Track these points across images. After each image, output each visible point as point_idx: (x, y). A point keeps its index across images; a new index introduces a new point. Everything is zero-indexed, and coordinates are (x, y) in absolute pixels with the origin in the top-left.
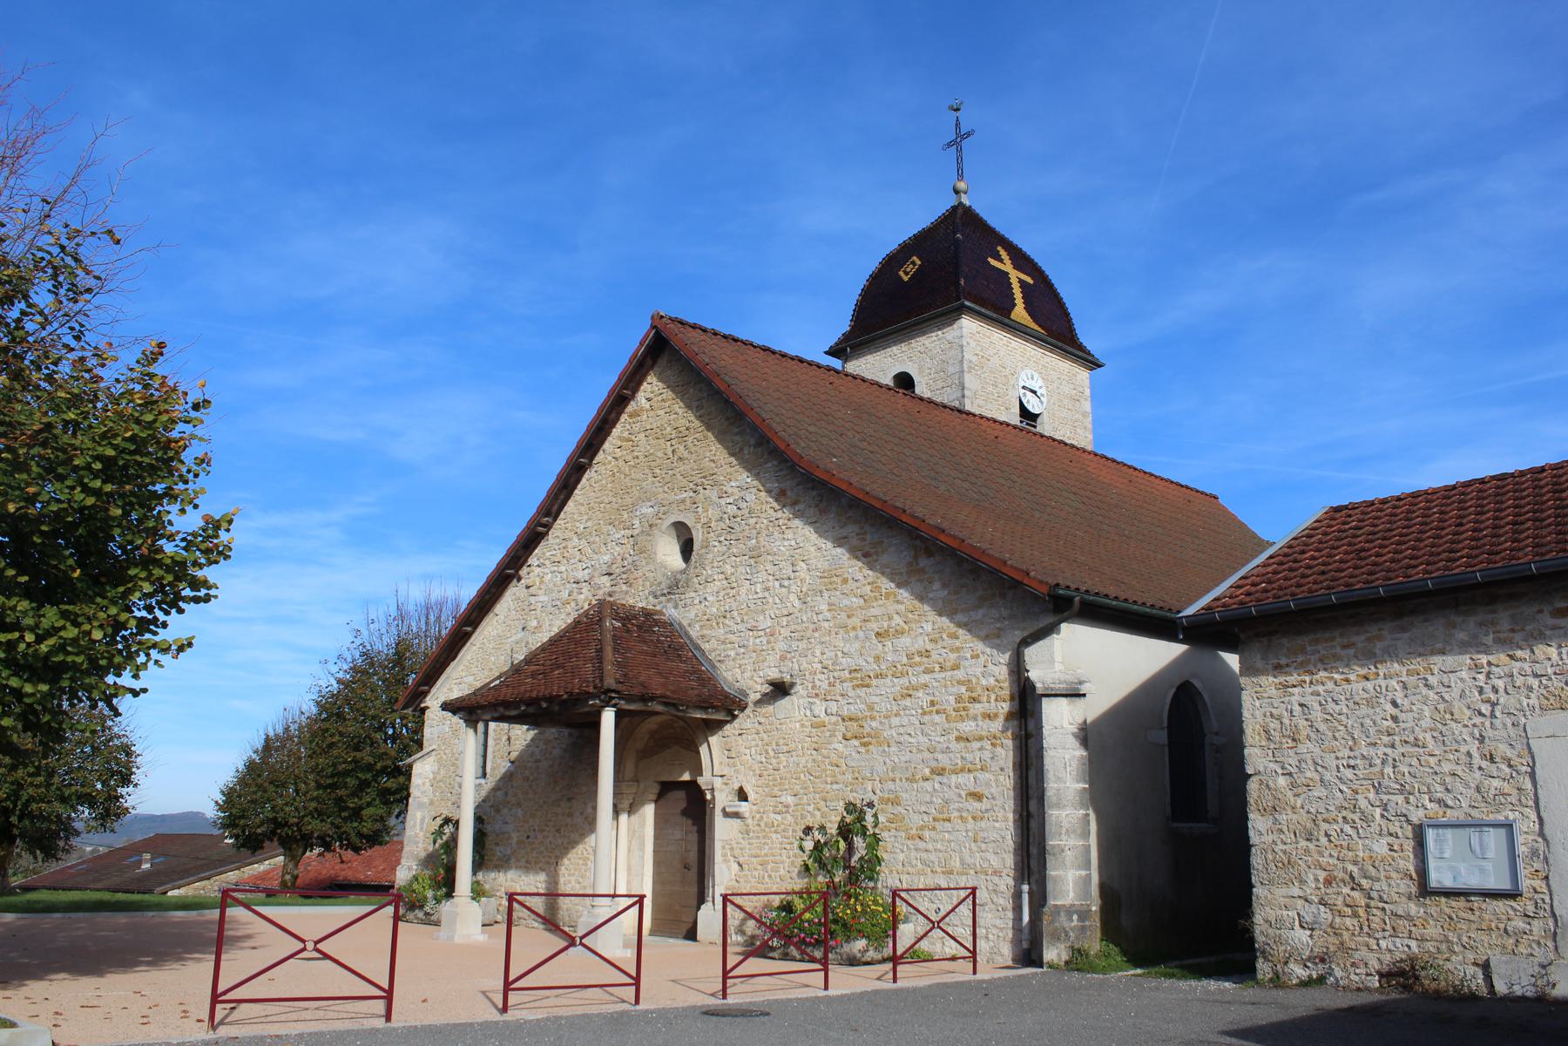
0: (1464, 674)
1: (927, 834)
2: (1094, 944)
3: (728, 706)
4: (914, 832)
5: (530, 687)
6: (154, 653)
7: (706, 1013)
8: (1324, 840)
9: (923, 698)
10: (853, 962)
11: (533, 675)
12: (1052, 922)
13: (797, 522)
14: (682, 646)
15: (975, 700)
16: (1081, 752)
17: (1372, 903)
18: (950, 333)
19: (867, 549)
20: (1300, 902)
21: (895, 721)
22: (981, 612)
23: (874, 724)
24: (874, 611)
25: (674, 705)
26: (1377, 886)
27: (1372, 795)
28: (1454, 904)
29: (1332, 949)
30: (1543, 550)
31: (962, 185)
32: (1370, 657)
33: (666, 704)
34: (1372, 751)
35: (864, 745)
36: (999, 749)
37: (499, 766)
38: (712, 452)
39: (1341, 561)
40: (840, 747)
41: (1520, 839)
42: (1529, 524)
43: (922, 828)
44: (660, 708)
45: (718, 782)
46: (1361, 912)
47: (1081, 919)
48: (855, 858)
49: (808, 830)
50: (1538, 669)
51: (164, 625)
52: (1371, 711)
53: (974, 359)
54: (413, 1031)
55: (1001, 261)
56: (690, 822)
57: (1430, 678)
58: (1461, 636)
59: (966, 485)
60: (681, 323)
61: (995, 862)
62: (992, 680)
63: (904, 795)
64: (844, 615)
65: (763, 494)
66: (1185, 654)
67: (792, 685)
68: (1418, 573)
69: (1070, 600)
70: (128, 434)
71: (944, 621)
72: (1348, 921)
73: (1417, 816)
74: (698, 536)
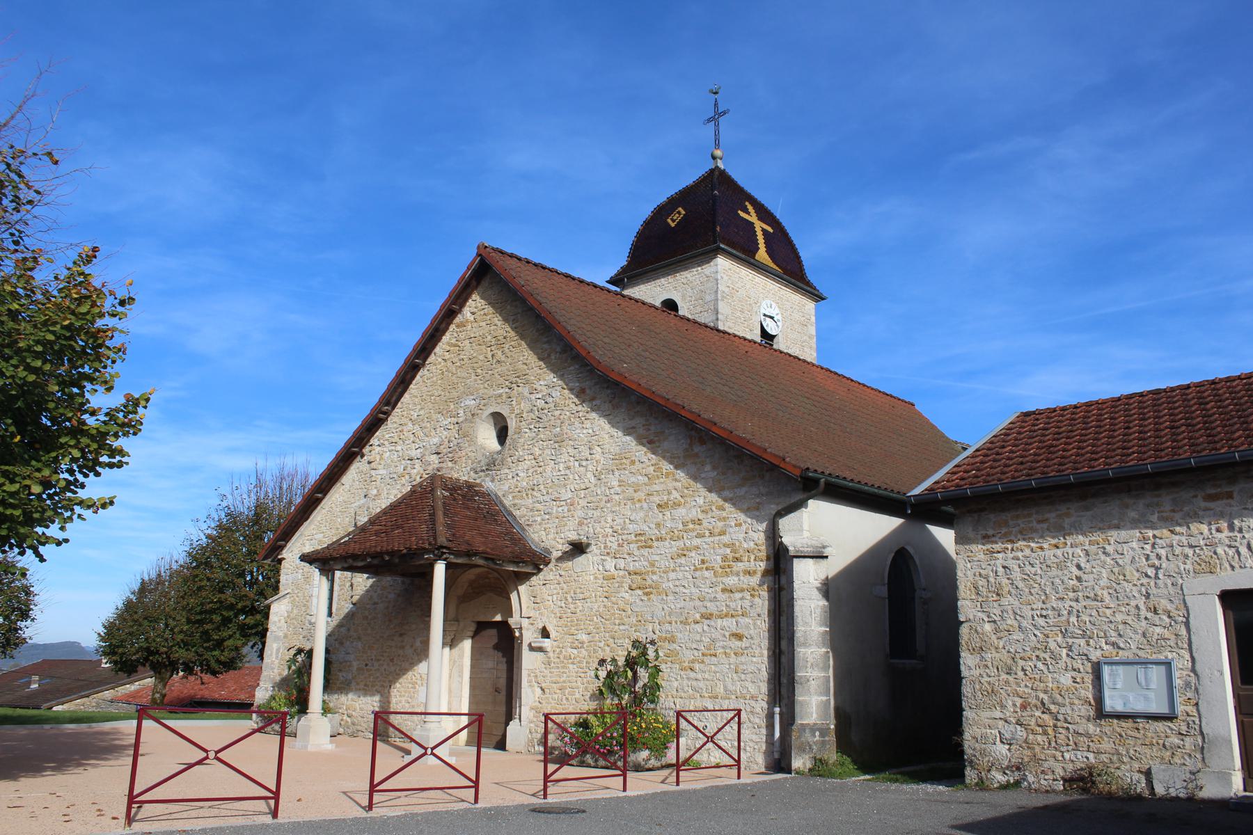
0: (1134, 545)
1: (697, 666)
2: (832, 756)
3: (535, 561)
4: (686, 664)
5: (374, 543)
6: (77, 509)
7: (534, 810)
8: (1021, 674)
9: (695, 557)
10: (638, 768)
11: (377, 533)
12: (799, 737)
13: (594, 415)
14: (498, 512)
15: (737, 560)
16: (824, 603)
17: (1059, 724)
18: (707, 269)
20: (1001, 723)
21: (672, 575)
22: (744, 489)
23: (655, 578)
24: (657, 487)
25: (492, 560)
26: (1063, 710)
27: (1059, 639)
28: (1124, 724)
29: (1026, 759)
30: (1199, 448)
31: (718, 153)
32: (1060, 530)
33: (486, 559)
34: (1060, 604)
35: (647, 594)
36: (757, 600)
37: (343, 607)
38: (525, 357)
39: (1035, 454)
40: (627, 596)
41: (1176, 674)
42: (1184, 428)
43: (693, 661)
44: (481, 562)
45: (525, 623)
46: (1050, 731)
47: (822, 735)
48: (640, 684)
49: (602, 662)
50: (1193, 541)
51: (83, 486)
52: (1060, 573)
53: (727, 290)
54: (297, 827)
55: (748, 213)
56: (500, 654)
57: (1107, 547)
58: (1133, 514)
59: (726, 389)
60: (501, 252)
61: (753, 689)
62: (752, 544)
63: (679, 635)
64: (631, 490)
65: (566, 391)
66: (901, 525)
67: (588, 545)
68: (1099, 465)
69: (817, 481)
70: (66, 323)
71: (713, 497)
72: (1039, 738)
73: (1095, 655)
74: (512, 425)
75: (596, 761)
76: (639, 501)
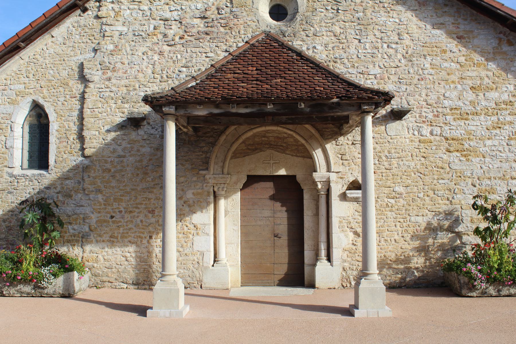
13: (400, 8)
19: (461, 34)
21: (489, 143)
40: (445, 157)
56: (278, 204)
64: (444, 73)
75: (499, 291)
76: (453, 82)
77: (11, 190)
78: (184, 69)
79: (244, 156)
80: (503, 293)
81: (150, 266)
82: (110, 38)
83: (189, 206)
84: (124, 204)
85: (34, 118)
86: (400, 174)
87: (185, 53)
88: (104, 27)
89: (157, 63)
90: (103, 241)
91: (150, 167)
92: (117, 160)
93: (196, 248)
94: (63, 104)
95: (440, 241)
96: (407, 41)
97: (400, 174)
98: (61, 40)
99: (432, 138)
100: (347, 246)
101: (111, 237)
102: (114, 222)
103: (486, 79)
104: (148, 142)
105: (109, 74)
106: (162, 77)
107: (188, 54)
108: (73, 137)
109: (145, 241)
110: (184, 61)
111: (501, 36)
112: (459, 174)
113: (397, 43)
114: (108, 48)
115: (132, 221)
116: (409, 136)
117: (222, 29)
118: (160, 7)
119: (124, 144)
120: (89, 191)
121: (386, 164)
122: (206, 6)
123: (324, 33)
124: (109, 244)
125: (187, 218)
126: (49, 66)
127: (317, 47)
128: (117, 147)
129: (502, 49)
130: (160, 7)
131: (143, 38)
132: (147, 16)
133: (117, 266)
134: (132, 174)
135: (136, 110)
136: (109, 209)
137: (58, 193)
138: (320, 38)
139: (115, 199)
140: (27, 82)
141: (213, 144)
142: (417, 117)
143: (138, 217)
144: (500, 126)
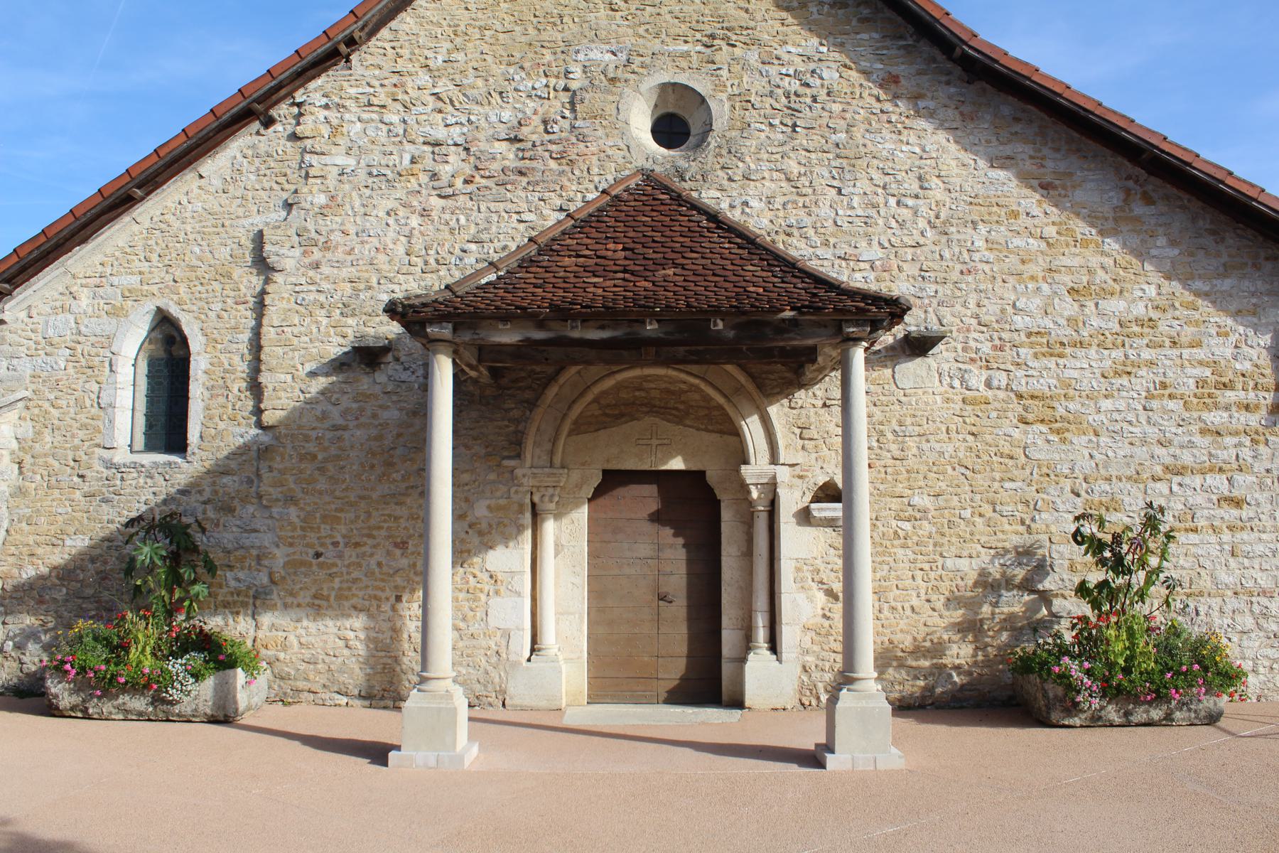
13: (922, 123)
19: (1048, 179)
21: (1106, 404)
40: (1016, 434)
56: (668, 531)
64: (1013, 259)
65: (854, 75)
75: (1127, 714)
76: (1032, 278)
77: (107, 495)
78: (473, 247)
79: (597, 430)
80: (1135, 718)
81: (396, 660)
82: (319, 181)
83: (481, 533)
84: (343, 529)
85: (159, 345)
86: (923, 468)
87: (475, 213)
88: (307, 157)
89: (416, 232)
90: (299, 605)
91: (399, 452)
92: (329, 435)
93: (493, 622)
94: (219, 317)
95: (1006, 610)
96: (937, 193)
97: (923, 468)
98: (217, 183)
99: (990, 394)
100: (811, 621)
101: (315, 597)
102: (321, 566)
103: (1100, 272)
104: (395, 398)
105: (317, 255)
106: (426, 263)
107: (482, 216)
108: (239, 385)
109: (386, 607)
110: (473, 230)
111: (1130, 184)
112: (1045, 470)
113: (917, 197)
114: (316, 201)
115: (359, 565)
116: (942, 389)
117: (553, 164)
118: (425, 117)
119: (346, 402)
120: (269, 500)
121: (894, 447)
122: (520, 115)
123: (766, 175)
124: (311, 611)
125: (476, 560)
126: (191, 237)
127: (751, 204)
128: (330, 407)
129: (1131, 210)
130: (425, 117)
131: (388, 181)
132: (397, 135)
133: (327, 659)
134: (362, 465)
135: (371, 331)
136: (312, 537)
137: (205, 503)
138: (758, 184)
139: (325, 518)
140: (146, 270)
141: (532, 404)
142: (959, 350)
143: (372, 555)
144: (1129, 369)
